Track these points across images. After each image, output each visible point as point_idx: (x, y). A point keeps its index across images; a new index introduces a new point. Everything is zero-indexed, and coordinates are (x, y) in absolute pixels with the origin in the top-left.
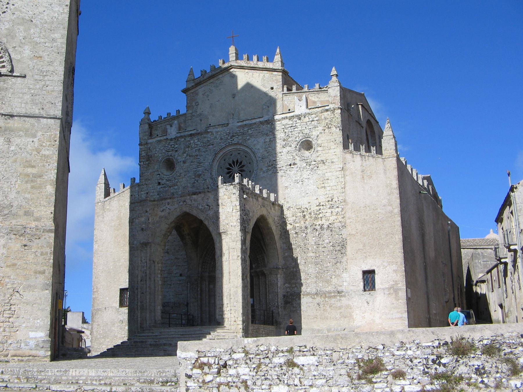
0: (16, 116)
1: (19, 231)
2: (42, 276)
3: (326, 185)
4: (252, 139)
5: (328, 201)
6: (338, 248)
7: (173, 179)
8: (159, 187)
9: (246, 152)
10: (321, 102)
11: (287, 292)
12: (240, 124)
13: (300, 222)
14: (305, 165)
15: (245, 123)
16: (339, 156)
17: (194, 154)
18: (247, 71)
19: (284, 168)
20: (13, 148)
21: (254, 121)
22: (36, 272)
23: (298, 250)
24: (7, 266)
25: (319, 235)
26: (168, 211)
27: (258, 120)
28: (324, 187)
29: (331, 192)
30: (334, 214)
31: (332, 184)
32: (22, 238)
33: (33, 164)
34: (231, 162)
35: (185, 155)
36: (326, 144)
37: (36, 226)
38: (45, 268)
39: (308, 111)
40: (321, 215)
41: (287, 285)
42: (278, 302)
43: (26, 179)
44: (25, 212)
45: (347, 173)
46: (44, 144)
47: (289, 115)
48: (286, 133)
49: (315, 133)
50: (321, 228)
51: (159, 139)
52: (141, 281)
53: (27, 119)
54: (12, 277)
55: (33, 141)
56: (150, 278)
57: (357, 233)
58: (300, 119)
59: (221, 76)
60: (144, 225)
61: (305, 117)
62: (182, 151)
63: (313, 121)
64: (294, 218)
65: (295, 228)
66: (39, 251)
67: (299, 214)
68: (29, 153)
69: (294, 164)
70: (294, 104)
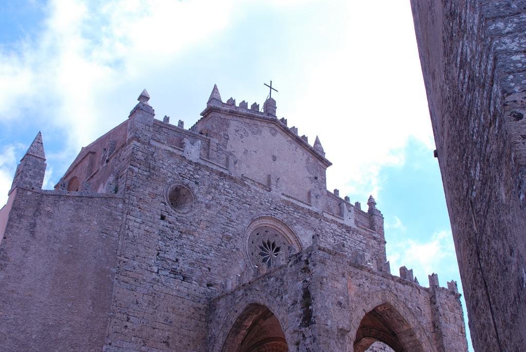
7: (188, 223)
8: (162, 222)
17: (222, 202)
18: (290, 139)
48: (335, 240)
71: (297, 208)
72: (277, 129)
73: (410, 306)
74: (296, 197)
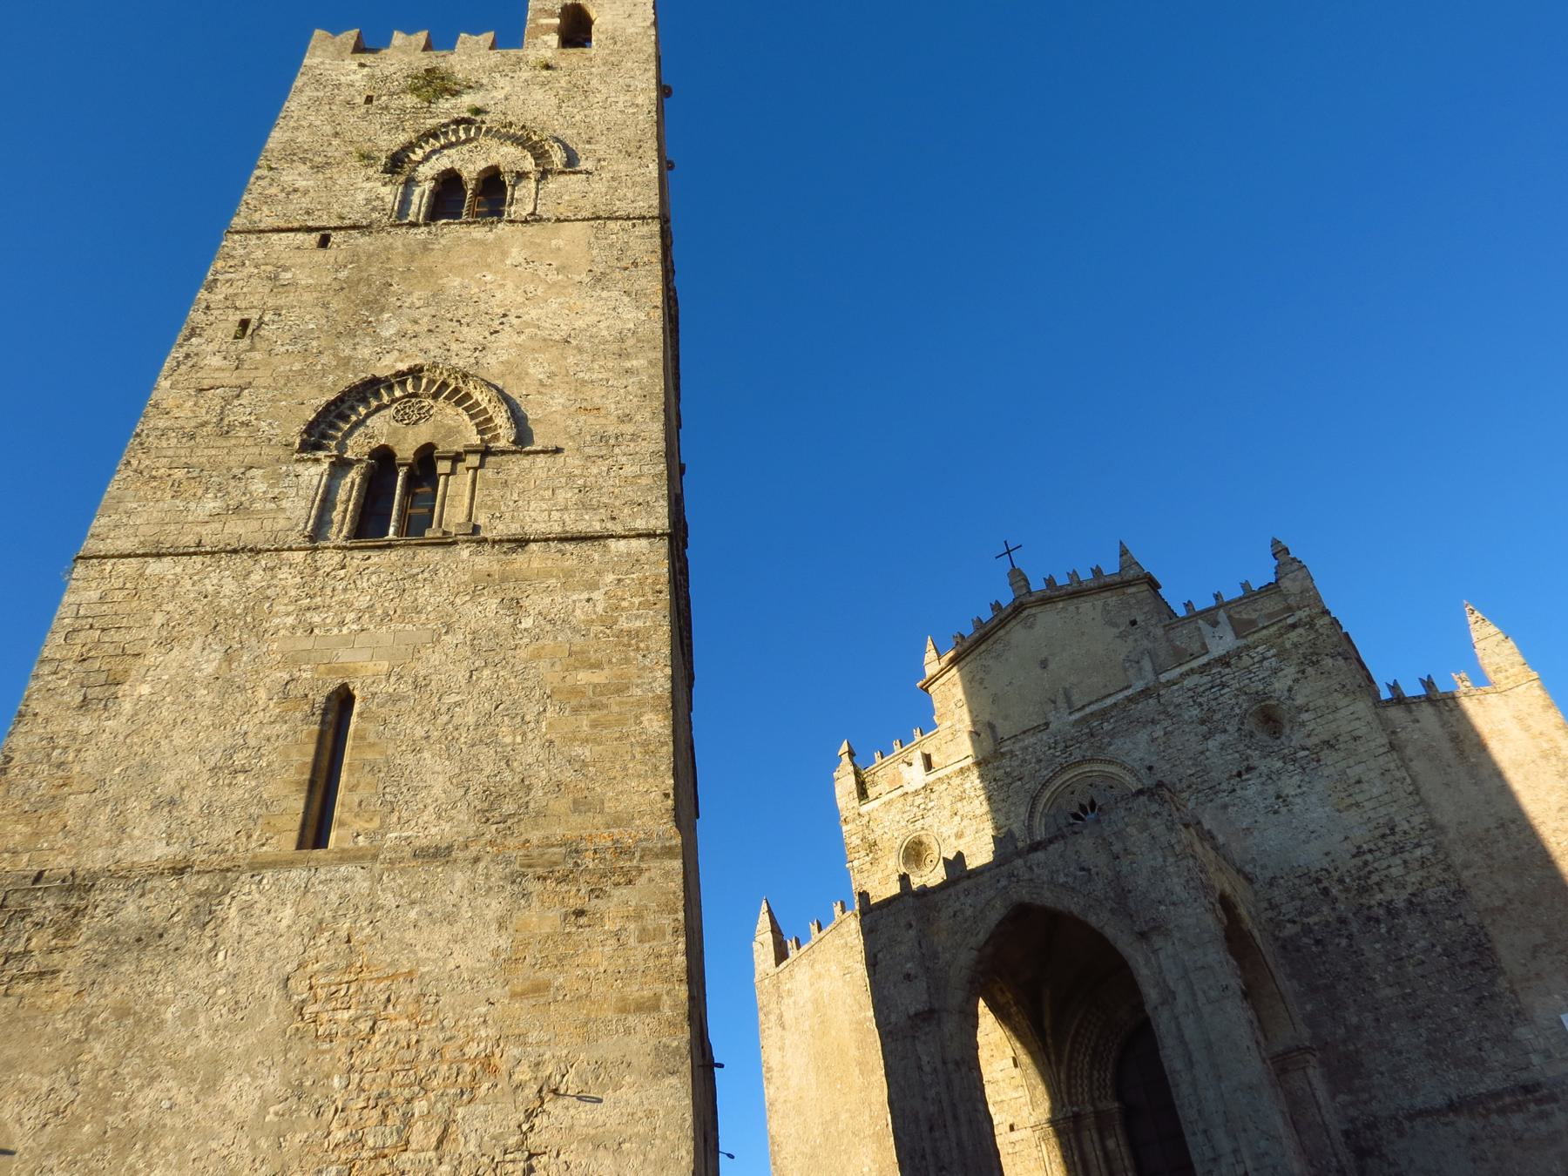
0: (535, 541)
1: (556, 863)
2: (650, 1020)
3: (1359, 798)
4: (1118, 742)
5: (1383, 836)
6: (1467, 957)
9: (1107, 776)
10: (1270, 616)
11: (1352, 1120)
12: (1077, 716)
13: (1318, 910)
14: (1280, 764)
15: (1088, 710)
16: (1370, 718)
18: (1061, 605)
19: (1224, 786)
20: (527, 623)
21: (1109, 701)
22: (623, 1010)
23: (1340, 988)
24: (513, 995)
25: (1389, 932)
26: (969, 912)
27: (1120, 696)
28: (1357, 805)
29: (1383, 811)
30: (1416, 865)
31: (1375, 792)
32: (564, 887)
33: (593, 657)
34: (1076, 810)
35: (957, 818)
36: (1321, 702)
37: (616, 842)
38: (660, 987)
39: (1241, 643)
40: (1375, 878)
41: (1341, 1098)
42: (1336, 1155)
43: (574, 702)
44: (575, 802)
45: (1410, 751)
46: (625, 604)
47: (1195, 664)
48: (1201, 705)
49: (1280, 685)
50: (1389, 911)
51: (885, 798)
52: (931, 1129)
53: (569, 547)
54: (533, 1037)
55: (588, 600)
56: (955, 1118)
57: (1510, 901)
58: (1228, 665)
59: (1002, 632)
60: (909, 965)
61: (1240, 658)
62: (947, 813)
63: (1265, 659)
64: (1298, 903)
65: (1307, 930)
66: (632, 926)
67: (1308, 890)
68: (579, 631)
69: (1249, 769)
70: (1201, 637)
71: (1103, 714)
72: (1033, 611)
73: (1062, 879)
74: (1104, 692)
